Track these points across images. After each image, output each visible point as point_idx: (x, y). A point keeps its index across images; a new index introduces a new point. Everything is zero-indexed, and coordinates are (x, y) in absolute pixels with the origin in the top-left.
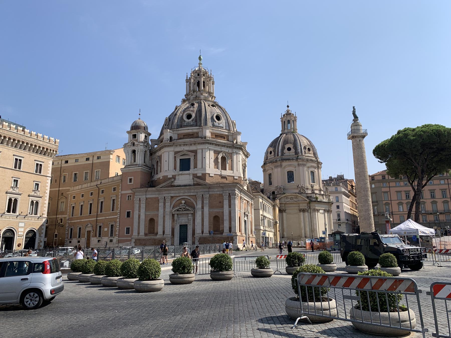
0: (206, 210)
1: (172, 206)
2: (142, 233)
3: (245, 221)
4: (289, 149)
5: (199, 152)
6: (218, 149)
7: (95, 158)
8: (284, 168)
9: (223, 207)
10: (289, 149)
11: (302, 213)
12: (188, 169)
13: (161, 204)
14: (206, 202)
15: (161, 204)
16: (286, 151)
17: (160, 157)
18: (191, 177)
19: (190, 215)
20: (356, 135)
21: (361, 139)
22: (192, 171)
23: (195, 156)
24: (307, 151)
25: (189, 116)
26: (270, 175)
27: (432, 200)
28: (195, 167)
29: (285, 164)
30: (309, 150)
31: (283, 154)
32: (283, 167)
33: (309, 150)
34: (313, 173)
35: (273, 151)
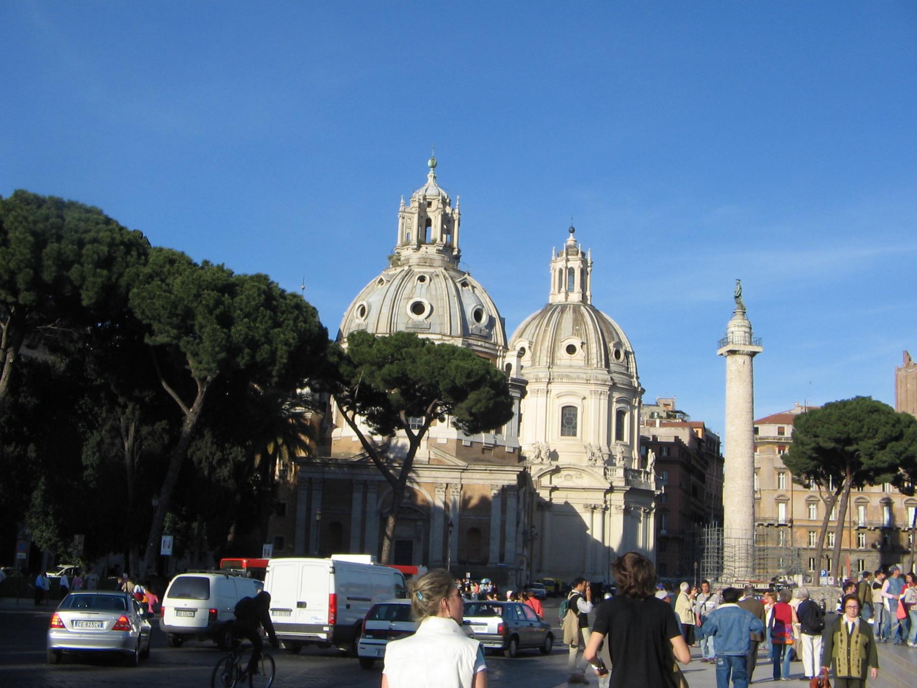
1: (380, 501)
4: (571, 349)
15: (357, 496)
16: (562, 352)
25: (418, 308)
35: (530, 347)
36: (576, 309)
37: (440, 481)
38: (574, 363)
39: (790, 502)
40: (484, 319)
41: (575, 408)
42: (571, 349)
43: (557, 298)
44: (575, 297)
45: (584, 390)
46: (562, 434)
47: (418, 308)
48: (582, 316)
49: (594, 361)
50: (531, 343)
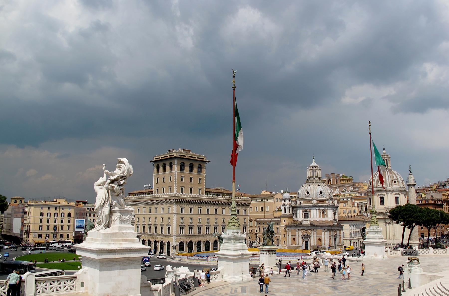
2: (290, 244)
3: (335, 239)
5: (312, 210)
8: (378, 195)
11: (387, 225)
13: (297, 233)
15: (297, 233)
17: (296, 210)
20: (408, 184)
22: (309, 219)
24: (393, 183)
25: (308, 193)
28: (311, 217)
30: (395, 182)
31: (377, 185)
33: (395, 182)
34: (397, 198)
45: (385, 193)
47: (308, 193)
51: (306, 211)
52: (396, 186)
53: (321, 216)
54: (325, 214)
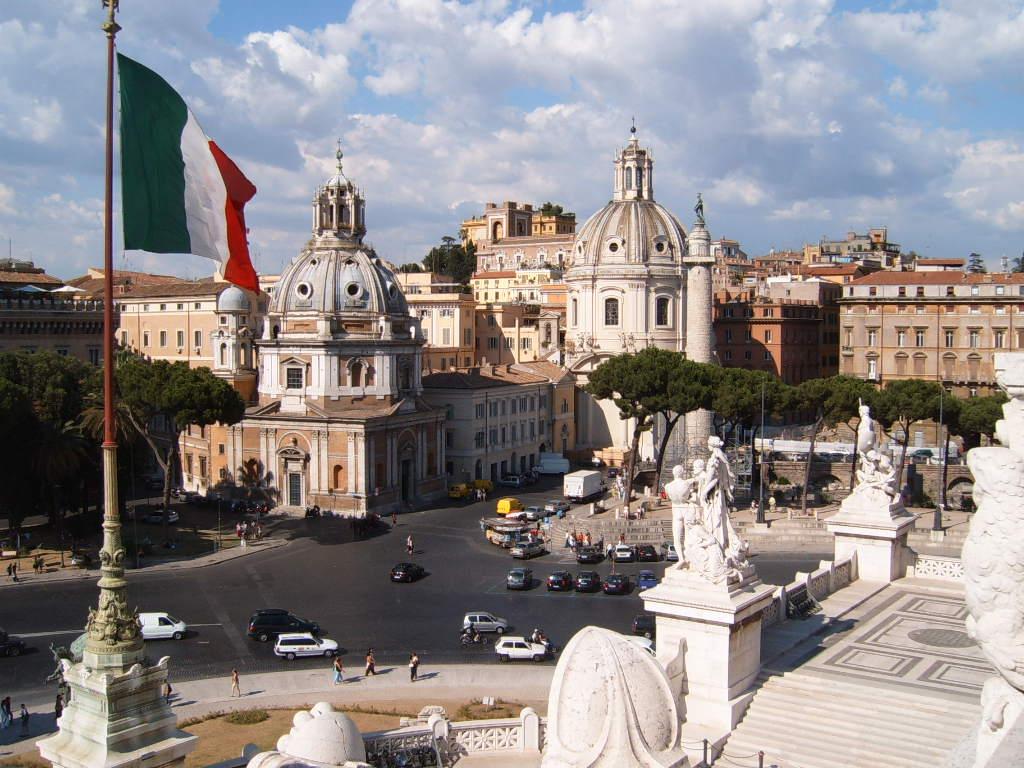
0: (324, 454)
3: (406, 464)
6: (347, 352)
7: (193, 305)
9: (346, 451)
10: (614, 247)
12: (300, 386)
14: (324, 442)
15: (263, 440)
16: (606, 251)
18: (303, 400)
19: (302, 461)
21: (702, 269)
23: (308, 365)
25: (303, 289)
26: (575, 300)
27: (971, 351)
29: (600, 284)
30: (660, 247)
32: (598, 290)
33: (660, 247)
36: (628, 205)
37: (314, 429)
38: (616, 260)
39: (880, 359)
40: (359, 293)
41: (616, 300)
42: (614, 247)
43: (618, 197)
44: (631, 194)
45: (624, 285)
46: (607, 323)
48: (630, 214)
49: (633, 257)
50: (584, 243)
51: (291, 360)
52: (664, 261)
53: (349, 379)
54: (364, 372)
